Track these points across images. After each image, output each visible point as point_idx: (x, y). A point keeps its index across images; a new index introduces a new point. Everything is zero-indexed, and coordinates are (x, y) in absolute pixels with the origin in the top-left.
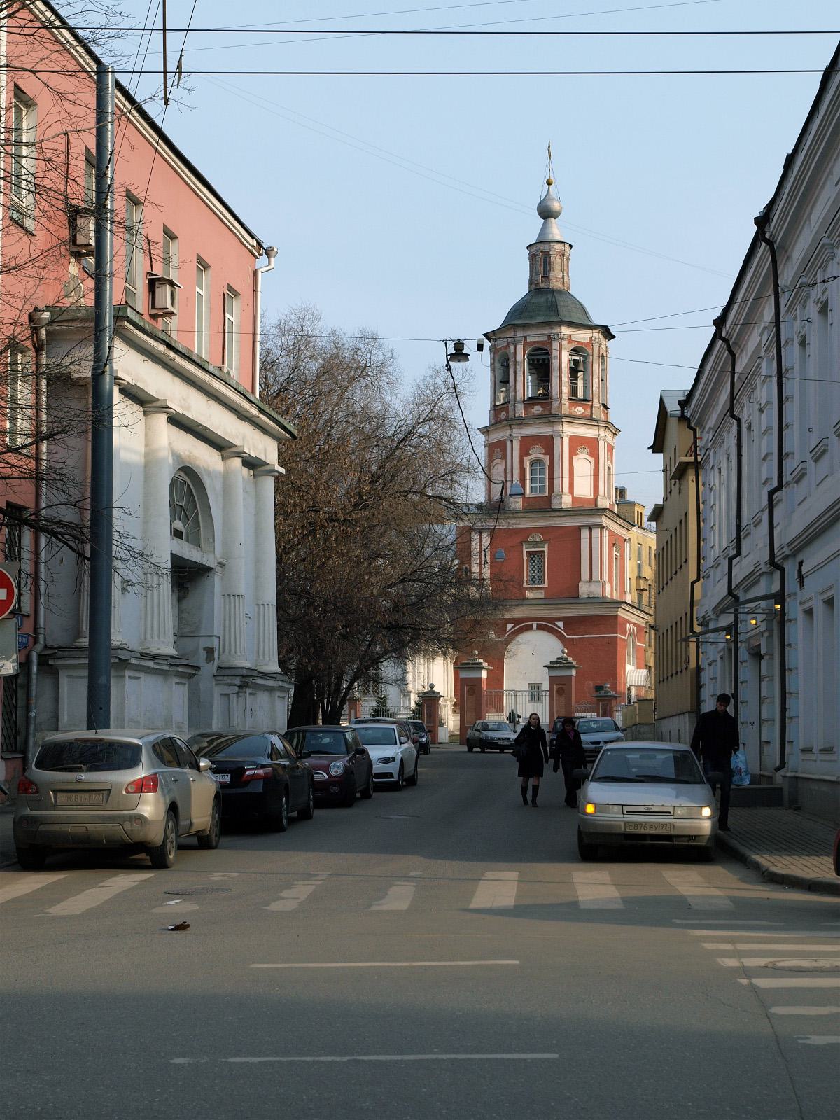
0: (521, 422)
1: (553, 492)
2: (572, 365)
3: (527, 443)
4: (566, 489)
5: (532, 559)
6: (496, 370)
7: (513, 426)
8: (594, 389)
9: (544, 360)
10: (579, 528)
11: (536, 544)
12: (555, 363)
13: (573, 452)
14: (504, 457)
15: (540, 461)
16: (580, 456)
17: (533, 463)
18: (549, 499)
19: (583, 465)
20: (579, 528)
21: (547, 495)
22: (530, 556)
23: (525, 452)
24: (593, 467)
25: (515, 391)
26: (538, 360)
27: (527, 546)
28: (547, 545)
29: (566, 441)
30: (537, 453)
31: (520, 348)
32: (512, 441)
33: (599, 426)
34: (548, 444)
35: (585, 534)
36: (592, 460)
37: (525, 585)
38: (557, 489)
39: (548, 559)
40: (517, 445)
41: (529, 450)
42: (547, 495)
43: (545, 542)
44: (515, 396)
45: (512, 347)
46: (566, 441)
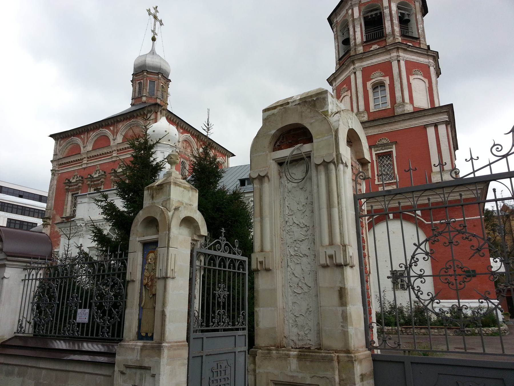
0: (362, 57)
1: (396, 103)
2: (400, 15)
3: (367, 73)
4: (407, 100)
5: (381, 160)
6: (339, 37)
7: (355, 62)
8: (420, 31)
9: (376, 14)
10: (425, 127)
11: (384, 145)
12: (387, 11)
13: (409, 73)
14: (350, 89)
15: (381, 84)
16: (416, 76)
17: (375, 87)
18: (393, 108)
19: (419, 86)
20: (425, 127)
21: (390, 107)
22: (379, 158)
23: (366, 79)
24: (427, 85)
25: (355, 39)
26: (372, 15)
27: (376, 149)
28: (394, 146)
29: (402, 63)
30: (377, 77)
31: (356, 10)
32: (355, 73)
33: (428, 55)
34: (386, 68)
35: (431, 131)
36: (426, 80)
37: (377, 182)
38: (399, 100)
39: (396, 157)
40: (359, 74)
41: (370, 76)
42: (390, 107)
43: (392, 143)
44: (355, 42)
45: (350, 12)
46: (402, 63)
